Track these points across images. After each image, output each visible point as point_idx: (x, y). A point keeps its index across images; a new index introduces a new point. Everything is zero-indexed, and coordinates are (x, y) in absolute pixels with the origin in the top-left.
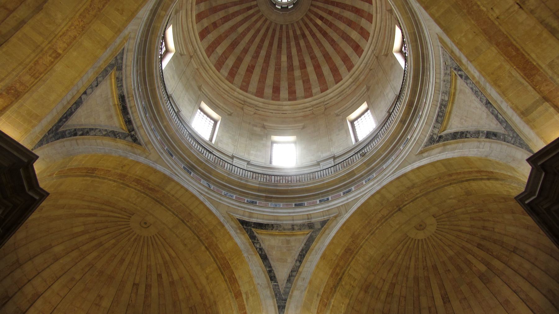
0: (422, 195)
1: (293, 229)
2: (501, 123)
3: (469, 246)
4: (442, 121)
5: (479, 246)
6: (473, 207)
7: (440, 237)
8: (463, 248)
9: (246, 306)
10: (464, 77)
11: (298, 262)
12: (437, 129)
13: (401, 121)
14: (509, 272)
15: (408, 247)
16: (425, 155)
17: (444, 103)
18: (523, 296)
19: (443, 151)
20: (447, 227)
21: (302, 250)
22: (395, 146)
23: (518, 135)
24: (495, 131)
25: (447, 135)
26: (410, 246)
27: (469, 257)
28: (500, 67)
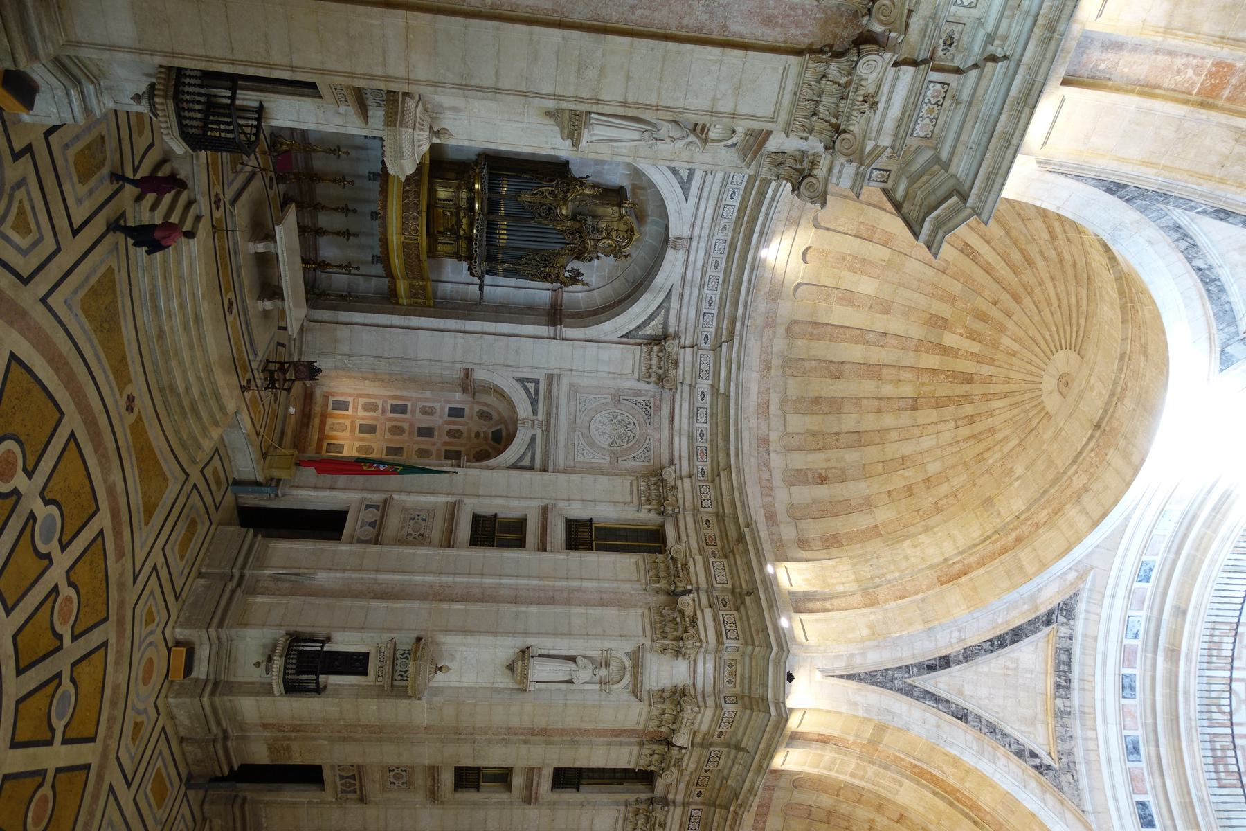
0: (1065, 473)
3: (985, 369)
4: (1057, 654)
5: (969, 378)
6: (991, 461)
7: (1034, 369)
8: (992, 362)
9: (1214, 116)
10: (1027, 754)
11: (1203, 266)
13: (1185, 612)
14: (909, 359)
15: (1071, 325)
16: (1072, 576)
17: (1062, 692)
18: (870, 336)
19: (1033, 598)
20: (1027, 396)
21: (1222, 289)
22: (1178, 553)
23: (884, 687)
24: (933, 674)
26: (1068, 328)
27: (976, 348)
28: (962, 780)
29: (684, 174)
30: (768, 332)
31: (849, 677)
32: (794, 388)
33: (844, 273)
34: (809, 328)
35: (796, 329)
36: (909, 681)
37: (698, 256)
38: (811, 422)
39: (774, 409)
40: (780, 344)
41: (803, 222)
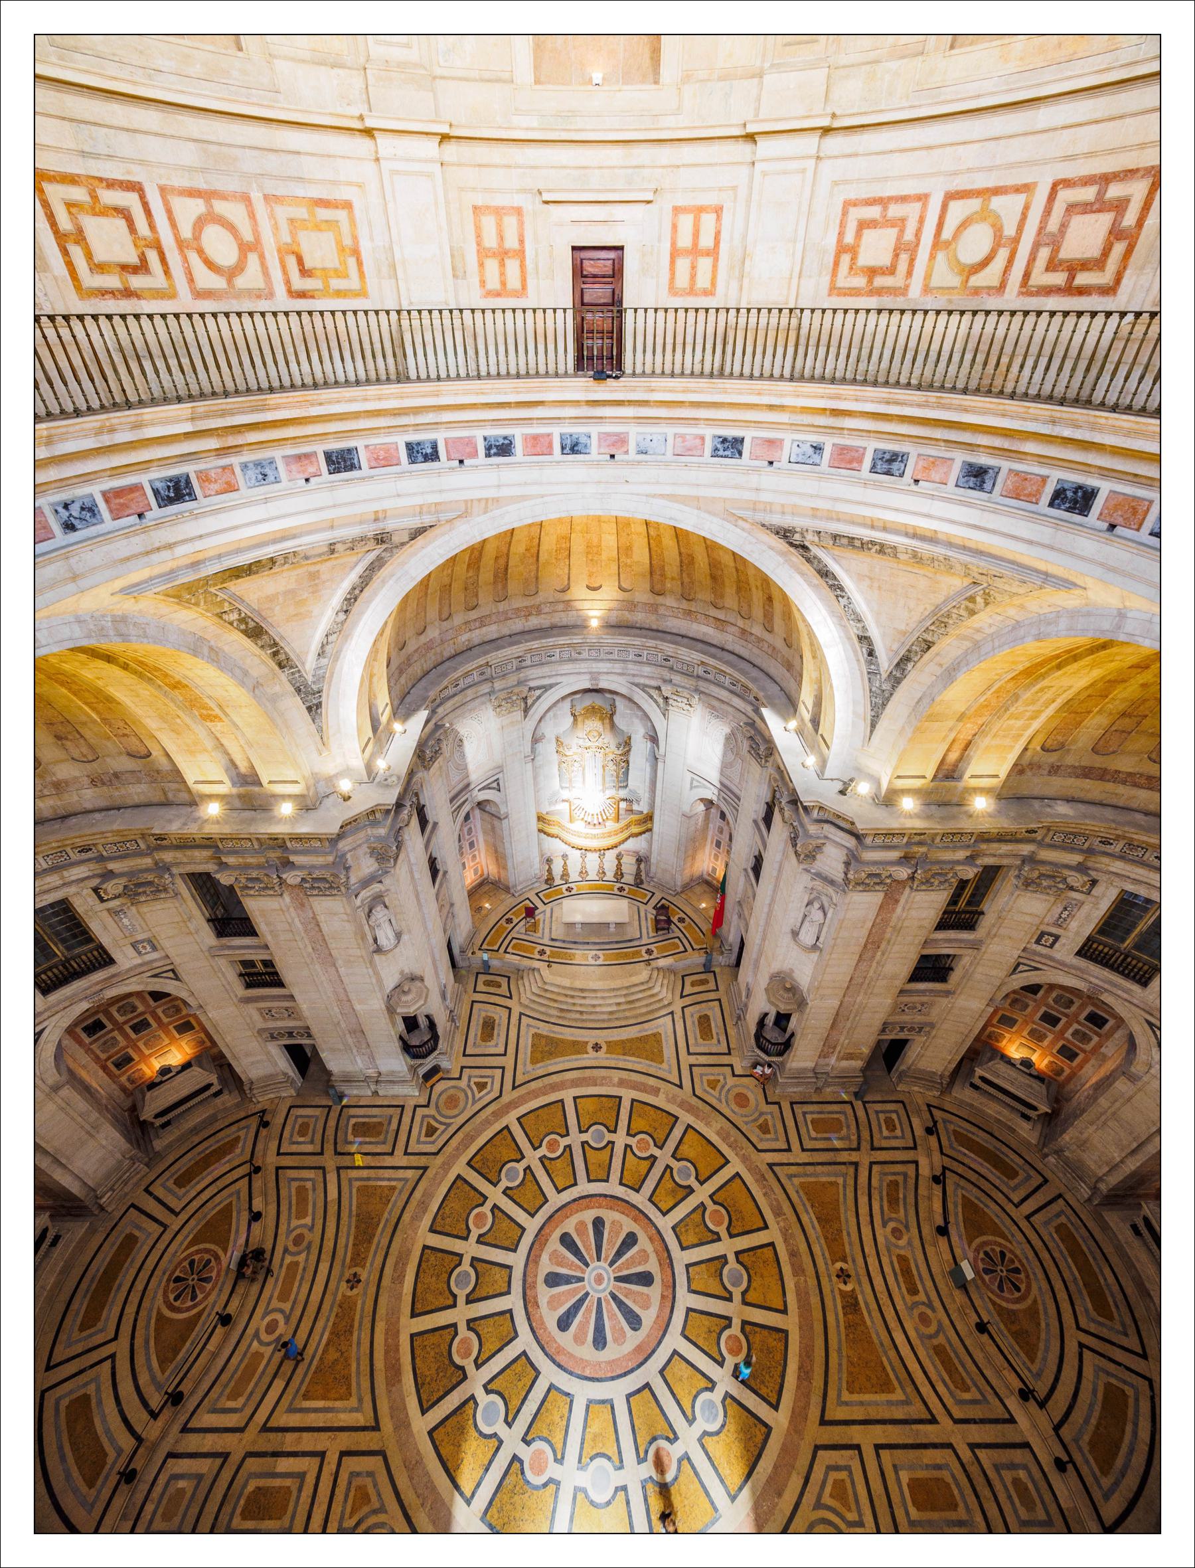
1: (333, 552)
2: (898, 665)
10: (971, 605)
12: (816, 539)
23: (888, 700)
25: (820, 561)
29: (538, 692)
30: (662, 611)
31: (873, 726)
32: (705, 595)
33: (604, 557)
34: (656, 577)
35: (658, 587)
36: (884, 676)
37: (603, 667)
38: (730, 590)
39: (721, 615)
40: (670, 601)
41: (567, 597)
